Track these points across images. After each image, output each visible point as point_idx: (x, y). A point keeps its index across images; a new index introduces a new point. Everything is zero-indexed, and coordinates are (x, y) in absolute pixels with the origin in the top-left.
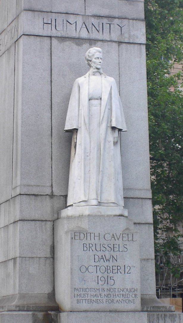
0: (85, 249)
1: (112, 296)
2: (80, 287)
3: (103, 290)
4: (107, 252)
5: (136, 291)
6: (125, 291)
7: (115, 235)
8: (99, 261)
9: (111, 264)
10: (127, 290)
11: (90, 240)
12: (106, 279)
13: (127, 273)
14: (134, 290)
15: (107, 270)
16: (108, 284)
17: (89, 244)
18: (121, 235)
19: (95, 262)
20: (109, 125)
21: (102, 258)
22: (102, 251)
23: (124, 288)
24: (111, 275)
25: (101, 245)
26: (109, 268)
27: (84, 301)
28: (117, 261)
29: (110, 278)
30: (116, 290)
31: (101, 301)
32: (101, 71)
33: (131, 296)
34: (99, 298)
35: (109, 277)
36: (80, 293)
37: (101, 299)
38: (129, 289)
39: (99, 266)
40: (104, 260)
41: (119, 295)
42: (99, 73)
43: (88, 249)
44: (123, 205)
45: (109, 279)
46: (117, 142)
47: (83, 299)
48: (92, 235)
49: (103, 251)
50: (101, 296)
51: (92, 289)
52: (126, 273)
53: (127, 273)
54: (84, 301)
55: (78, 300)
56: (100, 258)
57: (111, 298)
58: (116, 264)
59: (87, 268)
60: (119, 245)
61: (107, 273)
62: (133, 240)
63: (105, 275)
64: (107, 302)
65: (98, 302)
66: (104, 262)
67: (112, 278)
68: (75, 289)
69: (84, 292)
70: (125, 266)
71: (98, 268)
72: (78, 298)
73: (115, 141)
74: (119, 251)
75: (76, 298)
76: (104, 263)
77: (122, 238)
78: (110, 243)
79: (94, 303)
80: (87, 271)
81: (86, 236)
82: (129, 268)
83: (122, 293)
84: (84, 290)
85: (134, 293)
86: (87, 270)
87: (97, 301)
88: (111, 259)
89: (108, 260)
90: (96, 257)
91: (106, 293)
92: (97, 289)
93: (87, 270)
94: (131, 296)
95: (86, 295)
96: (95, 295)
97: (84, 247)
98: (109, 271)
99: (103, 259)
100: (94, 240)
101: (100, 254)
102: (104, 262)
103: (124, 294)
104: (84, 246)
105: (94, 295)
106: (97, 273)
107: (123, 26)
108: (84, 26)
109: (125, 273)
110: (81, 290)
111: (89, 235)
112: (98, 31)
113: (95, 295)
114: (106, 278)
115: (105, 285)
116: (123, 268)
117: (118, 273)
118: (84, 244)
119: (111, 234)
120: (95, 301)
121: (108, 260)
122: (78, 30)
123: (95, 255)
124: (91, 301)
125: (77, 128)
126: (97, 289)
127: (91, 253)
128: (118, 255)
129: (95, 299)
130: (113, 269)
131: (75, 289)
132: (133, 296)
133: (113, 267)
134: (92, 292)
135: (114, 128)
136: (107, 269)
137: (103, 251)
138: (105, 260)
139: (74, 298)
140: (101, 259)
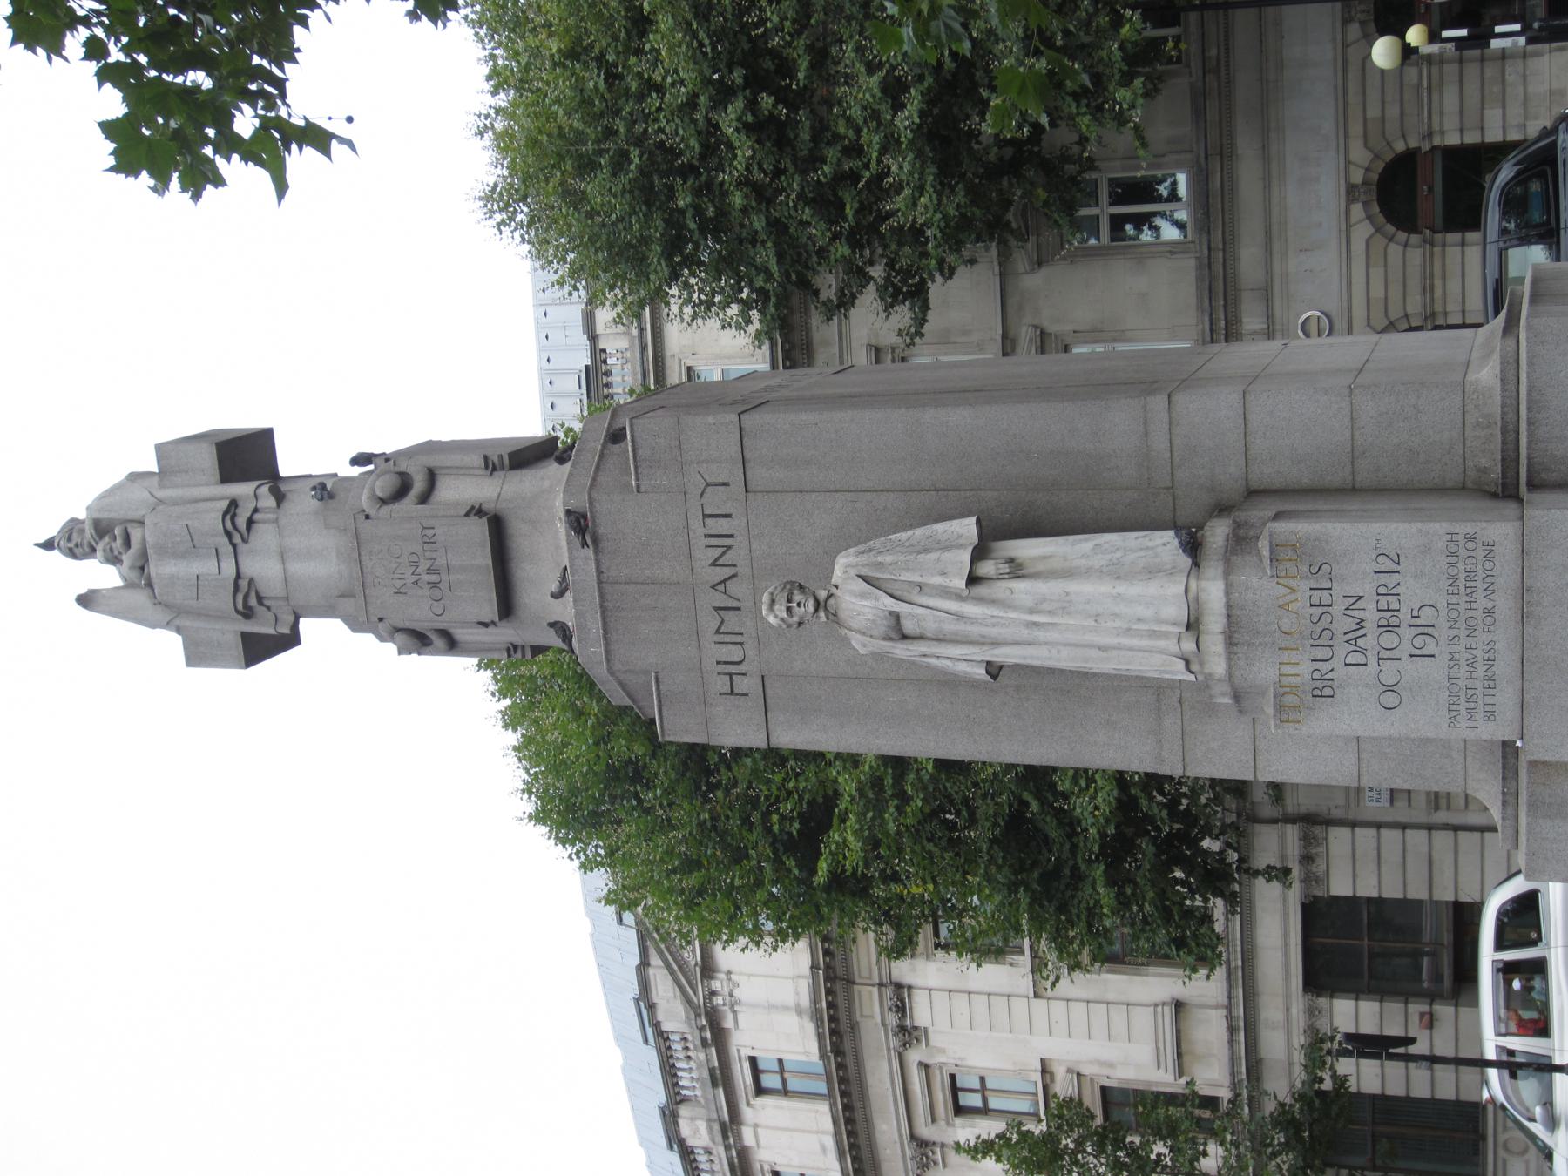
0: (1327, 691)
1: (1470, 613)
2: (1446, 710)
4: (1331, 627)
6: (1456, 570)
7: (1281, 602)
8: (1362, 651)
9: (1371, 616)
10: (1452, 565)
11: (1299, 678)
12: (1421, 630)
13: (1398, 564)
16: (1433, 626)
18: (1281, 581)
19: (1365, 665)
21: (1353, 642)
22: (1331, 643)
25: (1315, 643)
27: (1488, 700)
28: (1361, 597)
31: (1487, 648)
33: (1472, 554)
34: (1479, 653)
36: (1464, 712)
37: (1481, 647)
41: (1469, 590)
42: (828, 602)
43: (1330, 683)
45: (1418, 621)
46: (1011, 560)
47: (1481, 703)
48: (1288, 669)
52: (1398, 568)
53: (1398, 564)
54: (1488, 700)
57: (1478, 614)
59: (1385, 688)
61: (1398, 626)
63: (1407, 633)
64: (1491, 628)
66: (1364, 635)
69: (1463, 699)
70: (1376, 572)
72: (1480, 716)
73: (1008, 571)
74: (1330, 589)
75: (1480, 723)
76: (1369, 636)
78: (1308, 616)
79: (1493, 669)
80: (1395, 688)
82: (1381, 559)
83: (1461, 583)
84: (1455, 699)
85: (1462, 544)
89: (1358, 624)
90: (1350, 659)
91: (1463, 633)
94: (1472, 554)
98: (1394, 621)
99: (1355, 639)
101: (1341, 649)
102: (1364, 635)
108: (721, 587)
109: (1398, 572)
110: (1455, 707)
111: (1285, 681)
112: (729, 548)
114: (1415, 631)
116: (1384, 578)
117: (1398, 595)
119: (1280, 612)
121: (1358, 624)
122: (735, 604)
124: (1491, 682)
127: (1340, 673)
128: (1343, 594)
129: (1481, 668)
130: (1388, 610)
132: (1471, 545)
134: (1459, 675)
135: (973, 580)
136: (1389, 628)
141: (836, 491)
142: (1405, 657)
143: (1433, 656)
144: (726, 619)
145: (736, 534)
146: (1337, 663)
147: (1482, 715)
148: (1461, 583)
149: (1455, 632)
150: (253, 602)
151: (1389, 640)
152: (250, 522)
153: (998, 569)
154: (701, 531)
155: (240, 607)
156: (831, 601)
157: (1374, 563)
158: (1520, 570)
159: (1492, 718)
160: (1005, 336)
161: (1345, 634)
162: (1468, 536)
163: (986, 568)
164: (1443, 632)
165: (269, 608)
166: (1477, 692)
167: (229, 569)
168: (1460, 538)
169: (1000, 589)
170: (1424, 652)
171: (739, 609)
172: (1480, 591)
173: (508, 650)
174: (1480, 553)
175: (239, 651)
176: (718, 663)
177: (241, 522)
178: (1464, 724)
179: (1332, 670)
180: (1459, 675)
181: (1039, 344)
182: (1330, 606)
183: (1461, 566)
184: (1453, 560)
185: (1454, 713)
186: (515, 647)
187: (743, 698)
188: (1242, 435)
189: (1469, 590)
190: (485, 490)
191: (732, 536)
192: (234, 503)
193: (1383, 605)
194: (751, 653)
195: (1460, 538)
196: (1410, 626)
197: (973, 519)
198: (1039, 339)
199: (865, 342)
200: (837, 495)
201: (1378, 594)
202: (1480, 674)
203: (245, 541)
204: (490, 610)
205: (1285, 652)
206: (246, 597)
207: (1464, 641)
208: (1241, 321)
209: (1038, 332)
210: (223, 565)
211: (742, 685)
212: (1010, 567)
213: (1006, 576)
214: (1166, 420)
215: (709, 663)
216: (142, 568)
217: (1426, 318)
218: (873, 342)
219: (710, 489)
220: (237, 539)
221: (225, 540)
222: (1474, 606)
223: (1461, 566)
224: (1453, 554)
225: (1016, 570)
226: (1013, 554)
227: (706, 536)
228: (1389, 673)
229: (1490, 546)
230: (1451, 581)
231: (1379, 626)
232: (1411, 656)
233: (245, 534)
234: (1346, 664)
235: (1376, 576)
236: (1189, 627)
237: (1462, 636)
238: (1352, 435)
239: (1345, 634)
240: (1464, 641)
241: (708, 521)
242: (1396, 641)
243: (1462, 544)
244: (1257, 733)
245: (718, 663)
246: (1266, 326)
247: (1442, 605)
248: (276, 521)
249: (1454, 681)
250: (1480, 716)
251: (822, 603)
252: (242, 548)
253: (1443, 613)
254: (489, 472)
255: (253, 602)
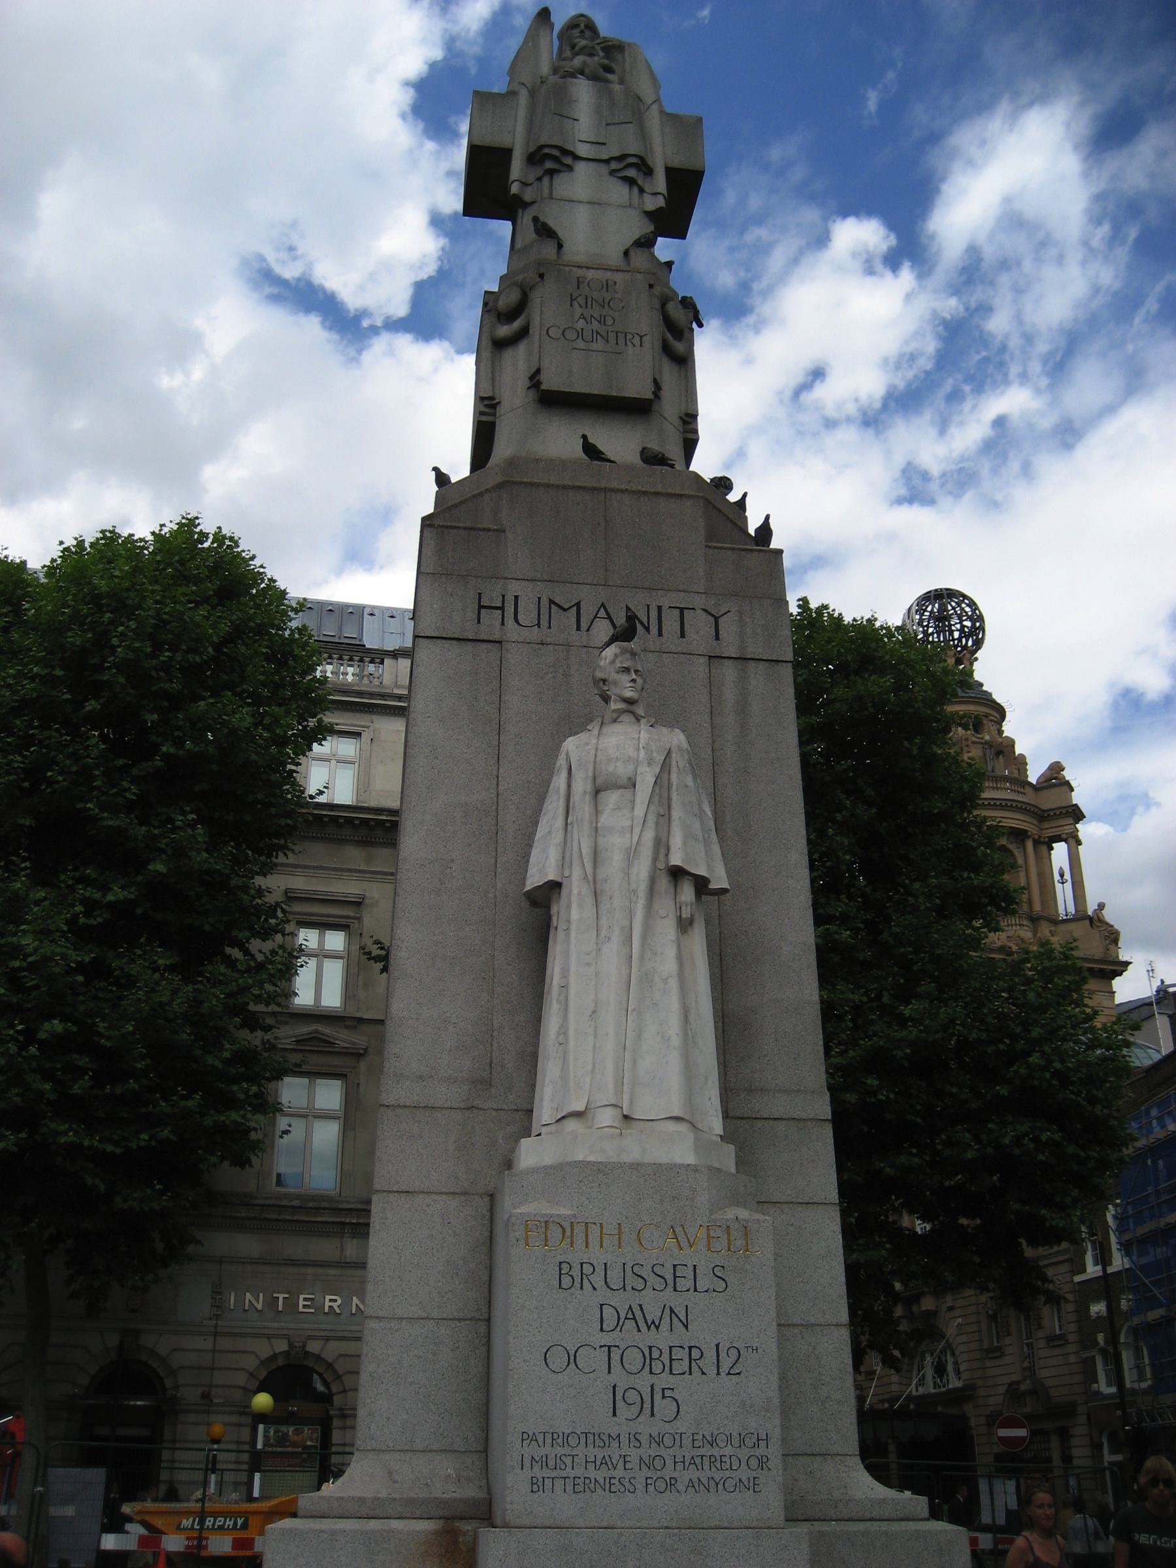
0: (566, 1281)
1: (670, 1463)
3: (635, 1438)
4: (648, 1291)
5: (762, 1443)
6: (722, 1445)
7: (678, 1230)
8: (619, 1327)
9: (663, 1339)
12: (647, 1398)
13: (729, 1374)
14: (754, 1440)
15: (651, 1363)
16: (652, 1415)
17: (582, 1264)
19: (602, 1330)
20: (661, 865)
21: (630, 1315)
22: (629, 1288)
23: (716, 1432)
24: (664, 1380)
25: (628, 1269)
26: (659, 1352)
27: (559, 1484)
28: (686, 1327)
29: (661, 1394)
30: (687, 1442)
31: (627, 1485)
32: (640, 711)
35: (658, 1390)
36: (542, 1452)
38: (735, 1434)
39: (618, 1346)
40: (636, 1323)
41: (698, 1460)
42: (631, 715)
43: (577, 1284)
44: (722, 1133)
46: (691, 922)
47: (555, 1474)
49: (633, 1288)
50: (628, 1466)
51: (591, 1437)
52: (723, 1374)
53: (729, 1374)
54: (559, 1484)
55: (535, 1480)
56: (623, 1316)
57: (668, 1473)
58: (680, 1336)
60: (695, 1266)
61: (651, 1373)
62: (750, 1247)
63: (643, 1382)
65: (613, 1488)
66: (639, 1331)
67: (668, 1393)
68: (525, 1436)
69: (560, 1451)
70: (717, 1346)
71: (615, 1356)
72: (537, 1472)
73: (684, 916)
74: (695, 1290)
75: (528, 1473)
77: (705, 1242)
79: (599, 1491)
81: (568, 1233)
82: (734, 1352)
83: (707, 1450)
84: (560, 1440)
86: (572, 1360)
87: (609, 1486)
88: (666, 1319)
89: (653, 1322)
90: (607, 1311)
91: (647, 1451)
92: (610, 1436)
93: (572, 1360)
95: (568, 1461)
96: (604, 1462)
97: (560, 1274)
98: (657, 1367)
99: (634, 1318)
100: (601, 1246)
101: (621, 1301)
102: (639, 1331)
103: (717, 1455)
104: (562, 1272)
105: (599, 1457)
106: (609, 1372)
107: (721, 614)
108: (602, 613)
109: (718, 1374)
110: (549, 1441)
111: (579, 1230)
113: (604, 1462)
115: (642, 1419)
116: (710, 1355)
117: (690, 1373)
118: (560, 1263)
120: (601, 1481)
121: (653, 1322)
122: (584, 626)
123: (602, 1305)
125: (560, 880)
126: (610, 1436)
130: (671, 1360)
131: (525, 1436)
132: (754, 1463)
133: (673, 1349)
134: (590, 1446)
135: (677, 874)
136: (649, 1357)
137: (633, 1288)
138: (641, 1323)
139: (518, 1471)
140: (626, 1318)
141: (713, 750)
142: (613, 1378)
143: (614, 1415)
144: (566, 613)
145: (663, 639)
146: (603, 1294)
147: (539, 1475)
148: (707, 1450)
149: (644, 1439)
150: (549, 165)
151: (634, 1360)
152: (631, 182)
153: (687, 906)
154: (666, 602)
155: (546, 151)
156: (633, 719)
157: (728, 1345)
158: (726, 1524)
159: (535, 1488)
160: (361, 1020)
161: (640, 1306)
162: (765, 1460)
163: (687, 892)
164: (646, 1427)
165: (539, 179)
166: (569, 1469)
167: (583, 150)
168: (762, 1450)
169: (665, 907)
170: (620, 1404)
171: (578, 629)
172: (697, 1474)
173: (492, 398)
174: (744, 1474)
175: (489, 139)
176: (516, 597)
177: (631, 173)
178: (528, 1450)
179: (594, 1288)
180: (590, 1446)
181: (351, 1051)
182: (675, 1290)
183: (728, 1451)
184: (736, 1443)
185: (540, 1440)
186: (494, 407)
187: (475, 616)
188: (789, 1199)
189: (698, 1460)
190: (670, 407)
191: (660, 634)
192: (648, 171)
193: (678, 1354)
194: (525, 634)
195: (762, 1450)
196: (652, 1387)
197: (726, 885)
198: (355, 1051)
199: (367, 894)
200: (710, 752)
201: (690, 1348)
202: (592, 1473)
203: (612, 173)
204: (551, 381)
205: (616, 1232)
206: (555, 159)
207: (634, 1455)
208: (354, 1238)
209: (361, 1051)
210: (587, 147)
211: (491, 620)
212: (686, 919)
213: (678, 914)
214: (804, 1115)
215: (514, 588)
216: (582, 73)
217: (342, 1409)
218: (367, 901)
219: (713, 619)
220: (614, 165)
221: (616, 154)
222: (679, 1466)
223: (728, 1451)
224: (742, 1441)
225: (684, 925)
226: (696, 925)
227: (660, 608)
228: (593, 1359)
229: (753, 1485)
230: (709, 1439)
231: (650, 1348)
232: (614, 1387)
233: (620, 175)
234: (602, 1305)
235: (713, 1346)
236: (626, 1117)
237: (641, 1451)
238: (793, 1325)
239: (640, 1306)
240: (634, 1455)
241: (677, 612)
242: (634, 1369)
243: (759, 1452)
244: (434, 1197)
245: (516, 597)
246: (348, 1260)
247: (681, 1426)
248: (630, 206)
249: (583, 1440)
250: (537, 1472)
251: (631, 708)
252: (604, 170)
253: (668, 1428)
254: (682, 416)
255: (549, 165)
